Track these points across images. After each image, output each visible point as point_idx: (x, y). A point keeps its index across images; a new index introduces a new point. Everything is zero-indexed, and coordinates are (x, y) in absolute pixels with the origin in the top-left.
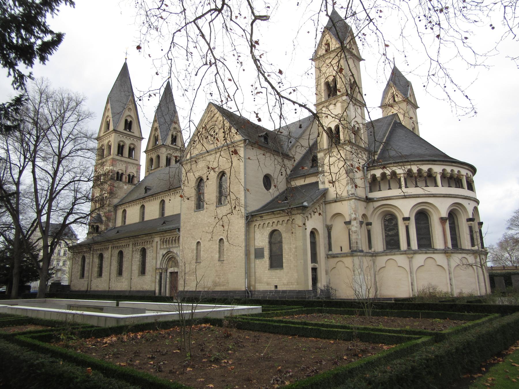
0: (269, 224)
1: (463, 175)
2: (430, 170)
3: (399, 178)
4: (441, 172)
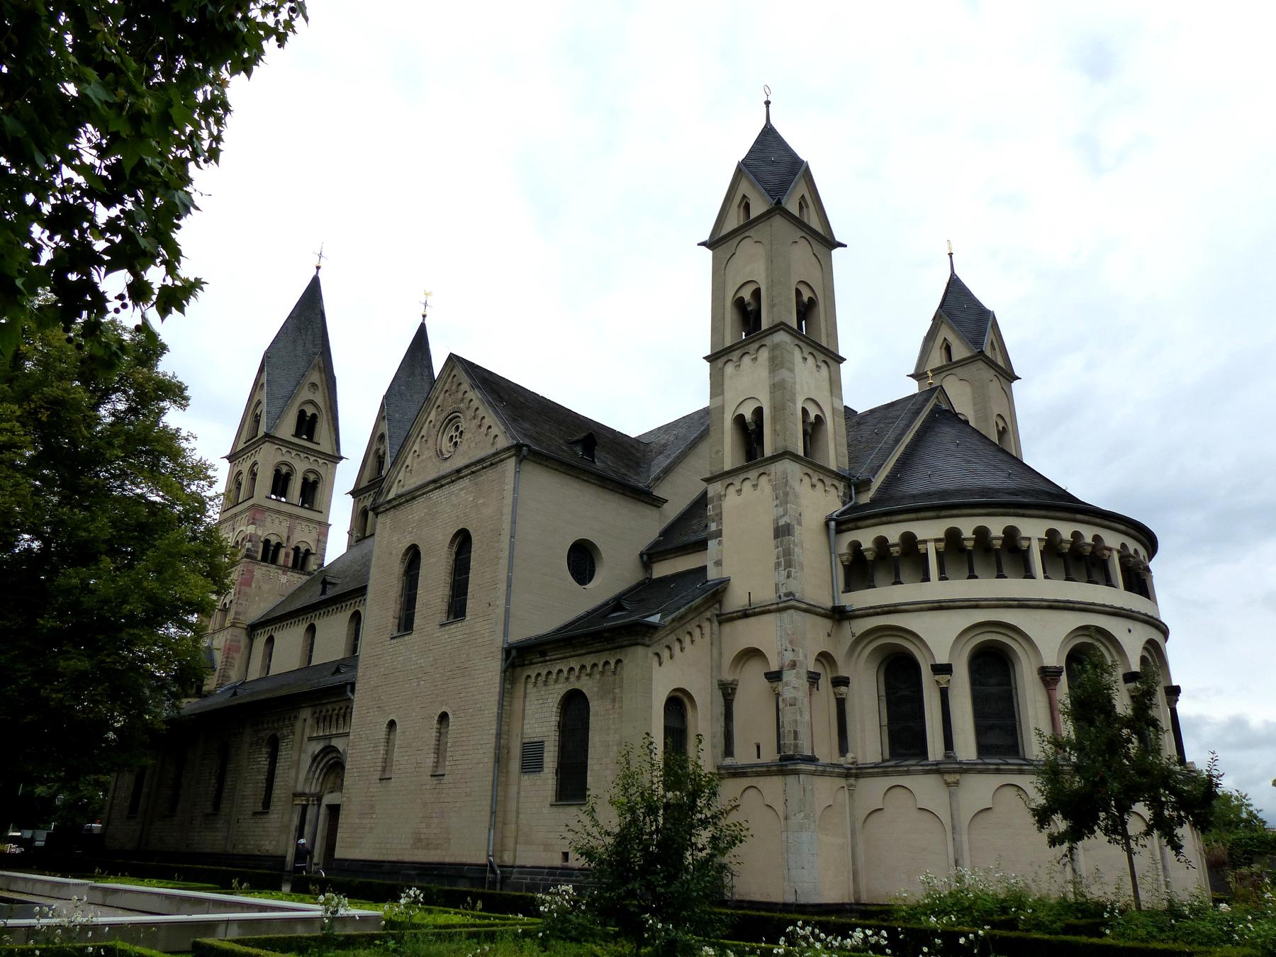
0: (561, 675)
1: (1110, 549)
2: (1011, 533)
3: (923, 551)
4: (1044, 536)
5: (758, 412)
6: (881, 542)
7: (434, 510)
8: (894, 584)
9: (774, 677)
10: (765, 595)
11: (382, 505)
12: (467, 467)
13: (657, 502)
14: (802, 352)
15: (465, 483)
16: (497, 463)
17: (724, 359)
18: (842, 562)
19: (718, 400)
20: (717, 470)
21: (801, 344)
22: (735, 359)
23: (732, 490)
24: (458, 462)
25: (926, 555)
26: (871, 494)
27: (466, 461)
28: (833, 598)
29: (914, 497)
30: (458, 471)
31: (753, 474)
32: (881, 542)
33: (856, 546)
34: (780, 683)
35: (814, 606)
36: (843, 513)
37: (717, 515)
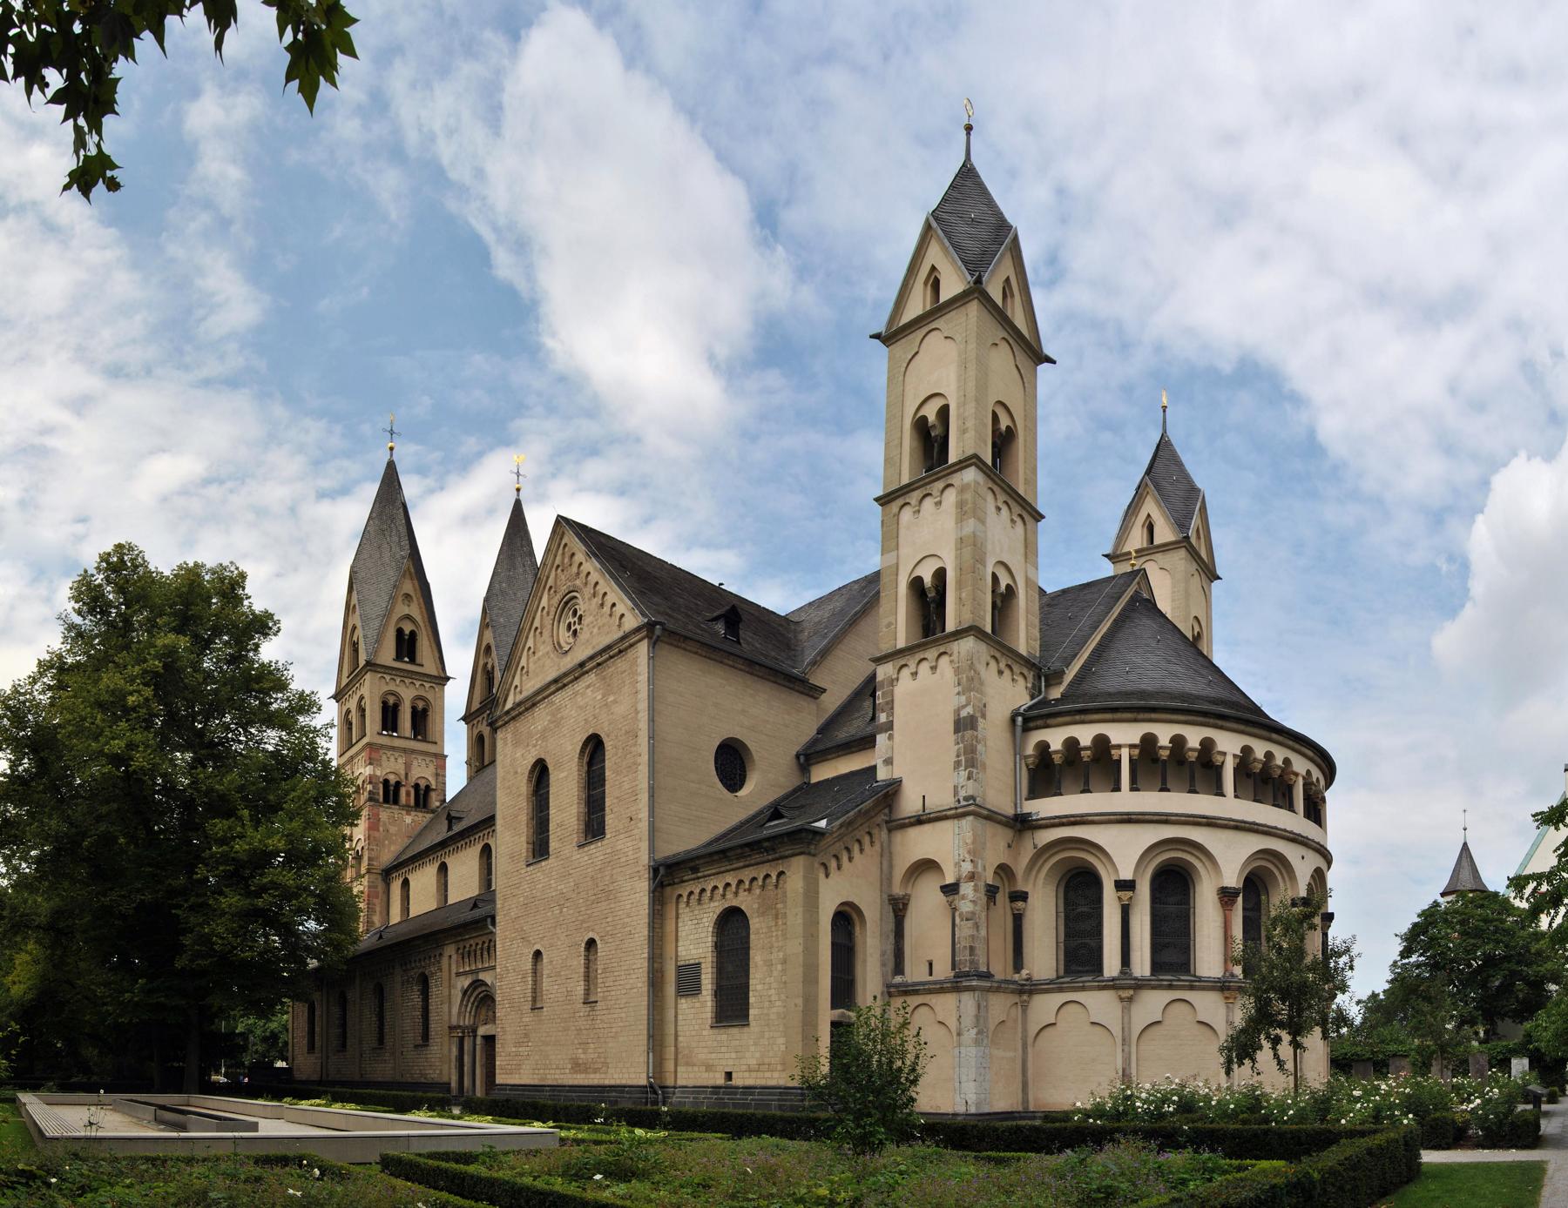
5: (940, 575)
6: (1072, 744)
7: (559, 716)
8: (1082, 792)
9: (950, 890)
10: (942, 799)
11: (500, 717)
12: (591, 658)
13: (814, 692)
14: (996, 499)
15: (591, 678)
16: (626, 649)
17: (900, 502)
18: (1027, 766)
19: (892, 555)
20: (886, 648)
21: (995, 488)
22: (914, 502)
23: (906, 672)
24: (581, 654)
25: (1119, 761)
26: (1062, 688)
27: (589, 652)
28: (1016, 805)
29: (1110, 694)
30: (582, 665)
31: (931, 654)
32: (1072, 744)
33: (1043, 747)
34: (956, 896)
35: (996, 813)
36: (1030, 708)
37: (887, 703)
